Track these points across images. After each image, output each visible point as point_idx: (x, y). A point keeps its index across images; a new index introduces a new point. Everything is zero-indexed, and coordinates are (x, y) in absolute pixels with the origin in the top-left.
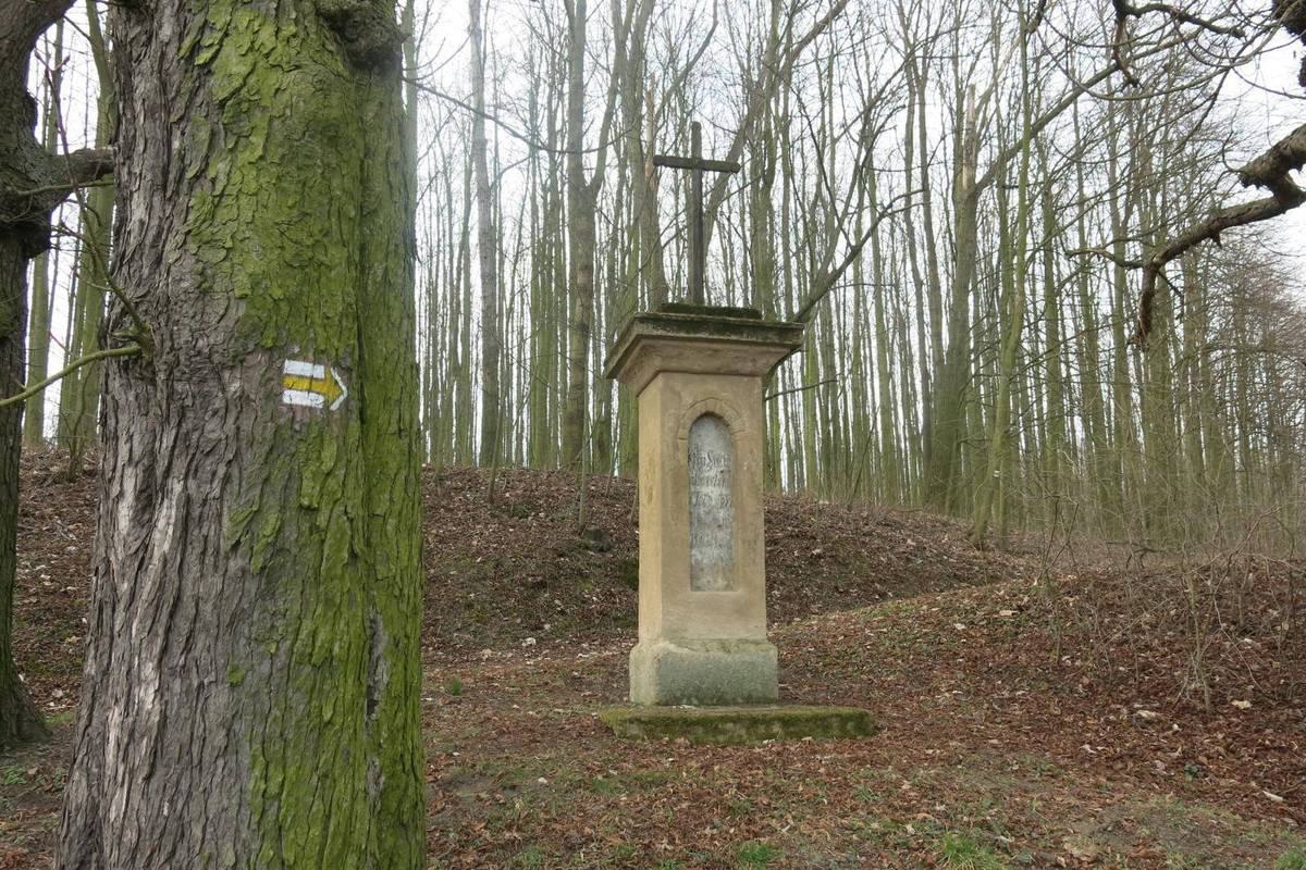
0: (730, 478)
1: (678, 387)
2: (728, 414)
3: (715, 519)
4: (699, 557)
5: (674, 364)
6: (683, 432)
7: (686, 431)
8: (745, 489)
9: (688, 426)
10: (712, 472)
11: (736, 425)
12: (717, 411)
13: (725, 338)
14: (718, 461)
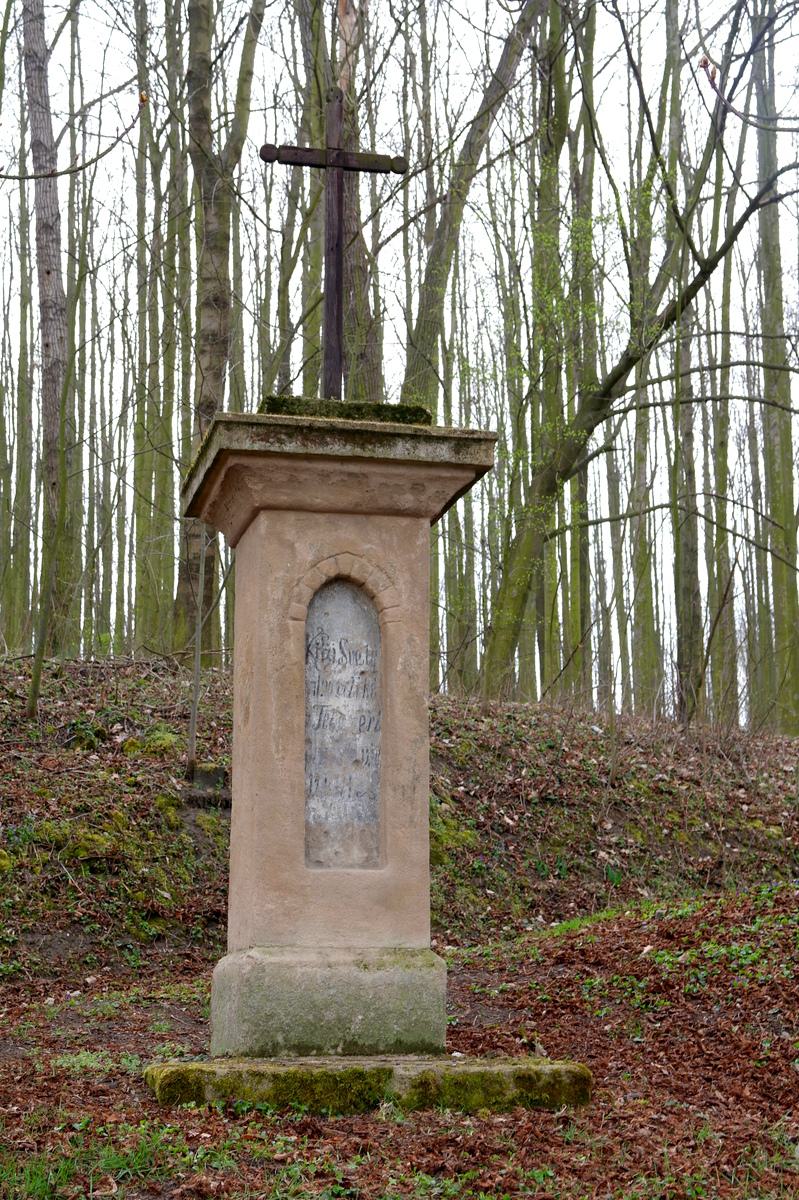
0: (376, 683)
1: (290, 535)
2: (373, 579)
4: (322, 812)
5: (283, 498)
6: (299, 608)
7: (303, 607)
8: (398, 700)
9: (307, 599)
10: (345, 673)
11: (385, 597)
12: (354, 574)
14: (356, 654)
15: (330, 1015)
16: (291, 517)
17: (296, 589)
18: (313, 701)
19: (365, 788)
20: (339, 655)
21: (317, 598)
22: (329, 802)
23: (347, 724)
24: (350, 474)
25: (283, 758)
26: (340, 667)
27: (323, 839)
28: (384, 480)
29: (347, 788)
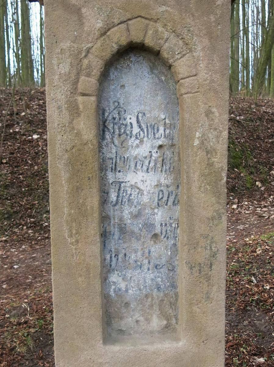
3: (149, 226)
4: (123, 285)
8: (196, 176)
9: (96, 72)
12: (149, 41)
14: (154, 128)
17: (86, 62)
18: (111, 177)
19: (164, 260)
20: (136, 130)
21: (112, 70)
22: (129, 275)
23: (145, 199)
25: (77, 241)
26: (137, 142)
27: (124, 310)
29: (146, 261)
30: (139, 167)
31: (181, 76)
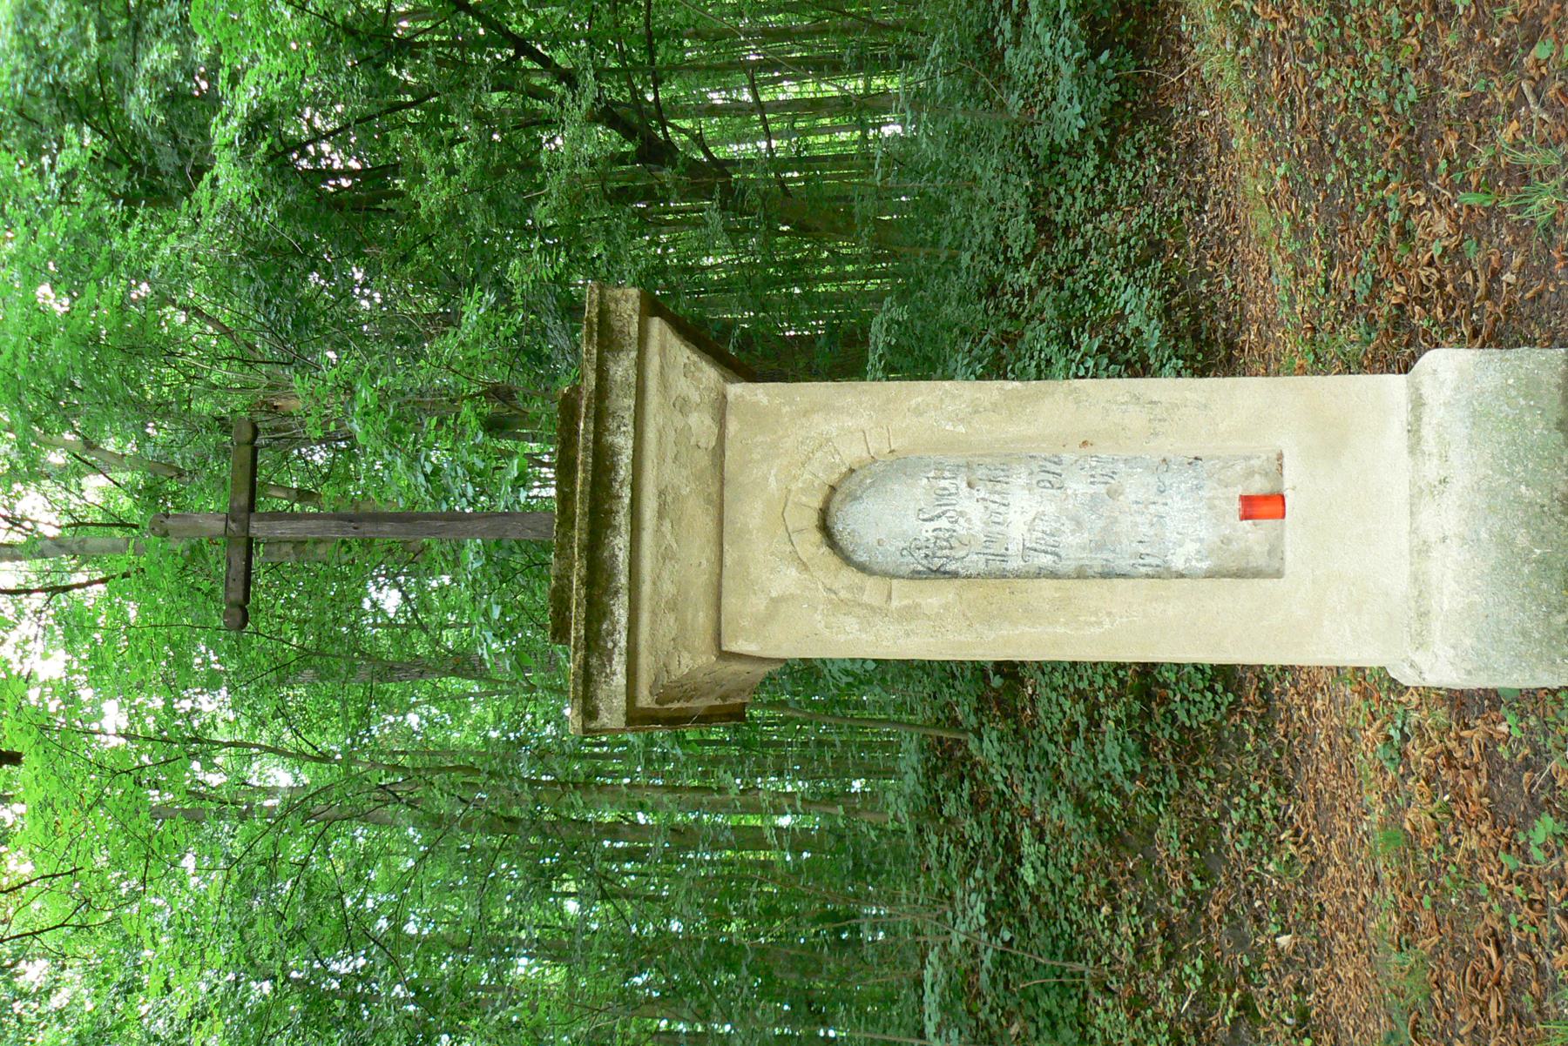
1: (759, 604)
2: (820, 473)
3: (1094, 503)
4: (1191, 547)
6: (872, 590)
7: (870, 582)
8: (1012, 430)
11: (852, 452)
13: (626, 493)
14: (942, 495)
15: (1522, 539)
16: (730, 603)
17: (843, 594)
18: (1015, 564)
19: (1153, 480)
20: (943, 523)
21: (855, 557)
23: (1051, 509)
24: (661, 515)
25: (1109, 614)
26: (961, 520)
27: (1234, 547)
28: (669, 460)
29: (1152, 507)
30: (1000, 519)
31: (865, 455)
